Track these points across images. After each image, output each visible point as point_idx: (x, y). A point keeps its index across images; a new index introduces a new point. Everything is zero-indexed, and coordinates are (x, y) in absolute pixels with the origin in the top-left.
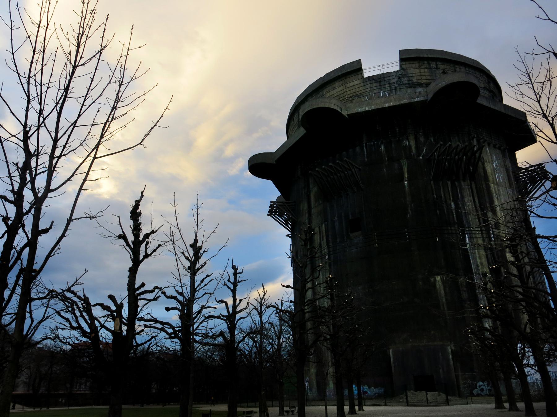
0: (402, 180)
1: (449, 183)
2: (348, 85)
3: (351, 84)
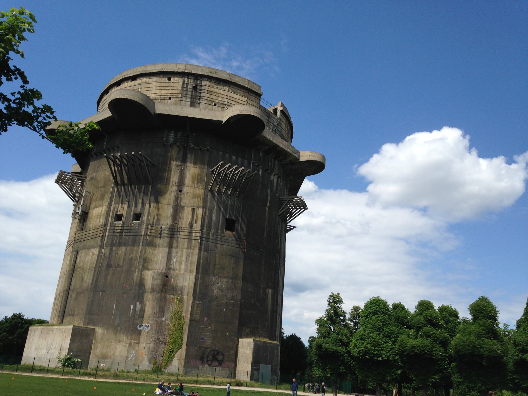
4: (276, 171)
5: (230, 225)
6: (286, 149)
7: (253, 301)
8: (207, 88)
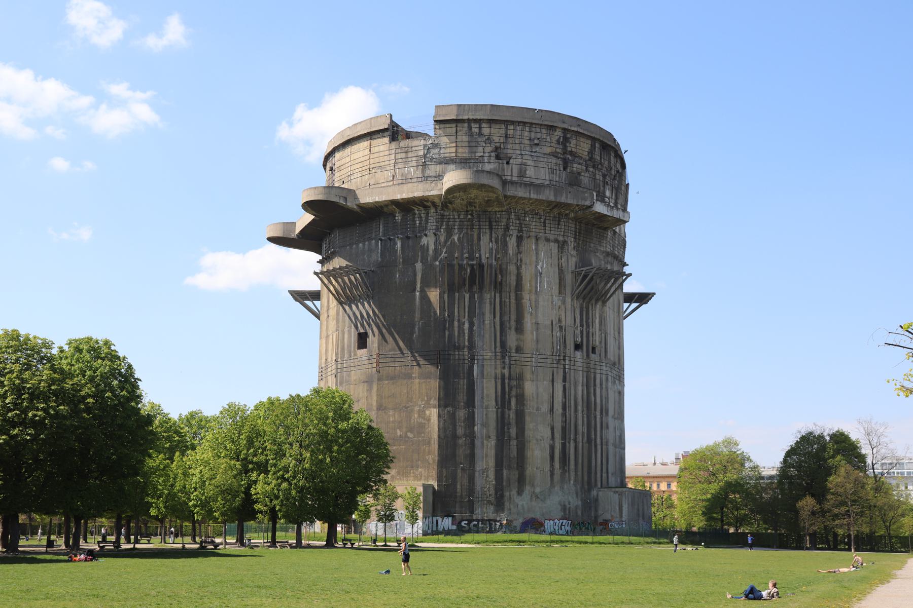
0: (414, 290)
1: (467, 296)
4: (432, 224)
5: (362, 341)
6: (411, 196)
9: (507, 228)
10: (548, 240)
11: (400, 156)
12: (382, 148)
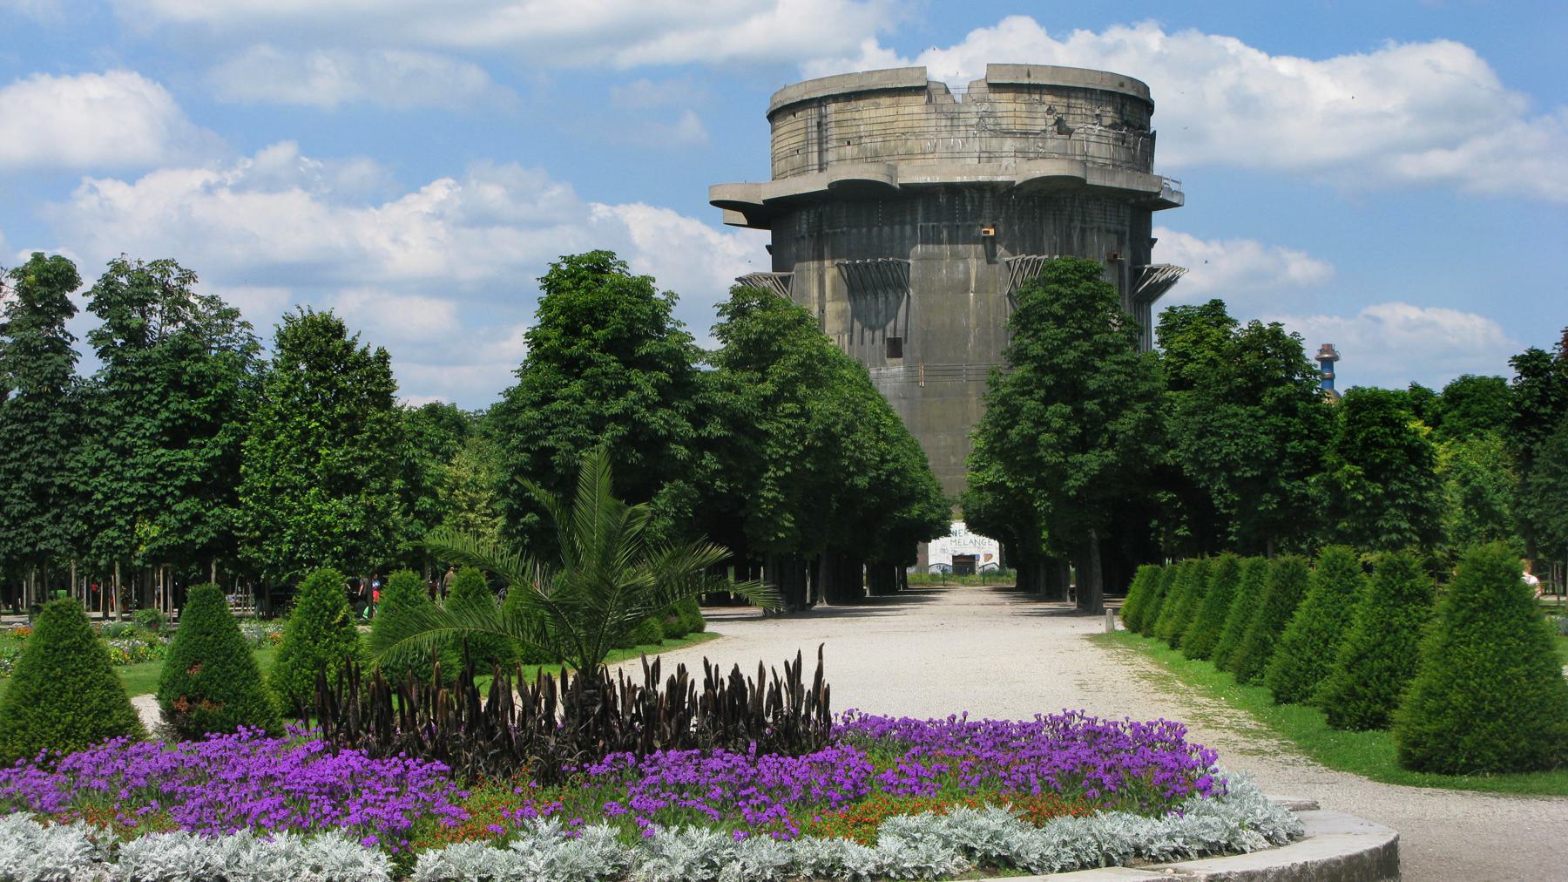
0: (967, 290)
2: (901, 111)
3: (908, 110)
6: (973, 179)
7: (953, 460)
8: (833, 117)
9: (1071, 220)
10: (1108, 231)
11: (943, 122)
12: (916, 109)
